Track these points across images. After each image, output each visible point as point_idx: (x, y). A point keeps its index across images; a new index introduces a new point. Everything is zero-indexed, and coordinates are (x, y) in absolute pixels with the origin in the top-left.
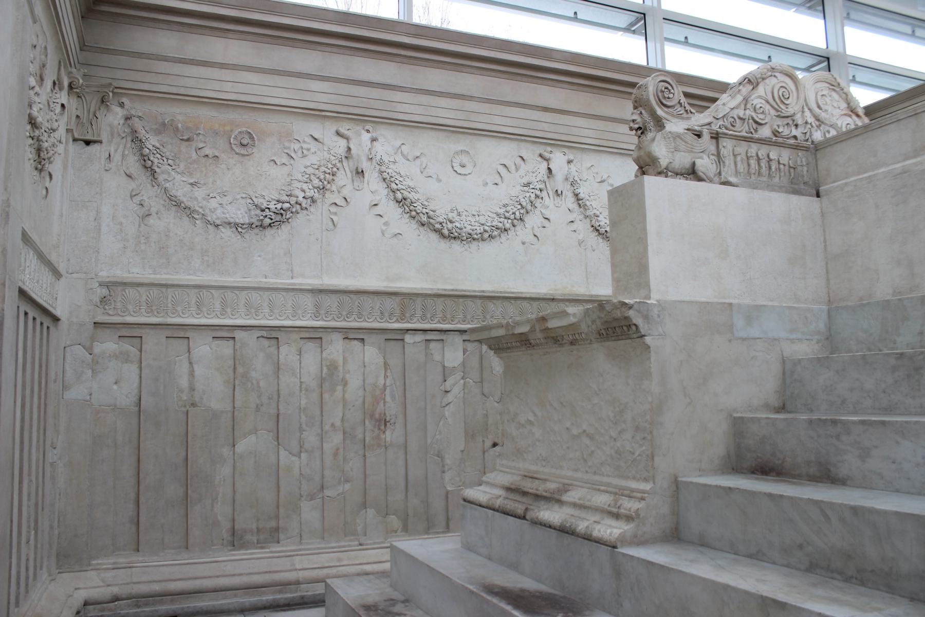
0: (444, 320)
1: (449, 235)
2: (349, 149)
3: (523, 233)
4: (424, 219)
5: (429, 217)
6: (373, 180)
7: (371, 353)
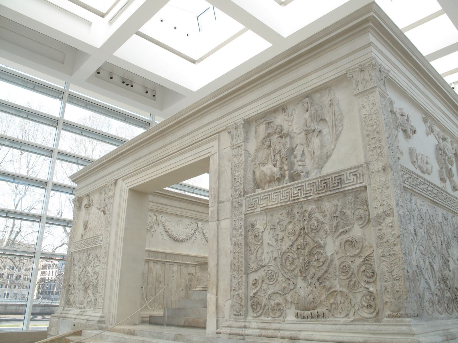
0: (174, 260)
1: (176, 240)
2: (157, 219)
3: (191, 241)
4: (171, 236)
5: (172, 236)
6: (161, 227)
7: (159, 266)
